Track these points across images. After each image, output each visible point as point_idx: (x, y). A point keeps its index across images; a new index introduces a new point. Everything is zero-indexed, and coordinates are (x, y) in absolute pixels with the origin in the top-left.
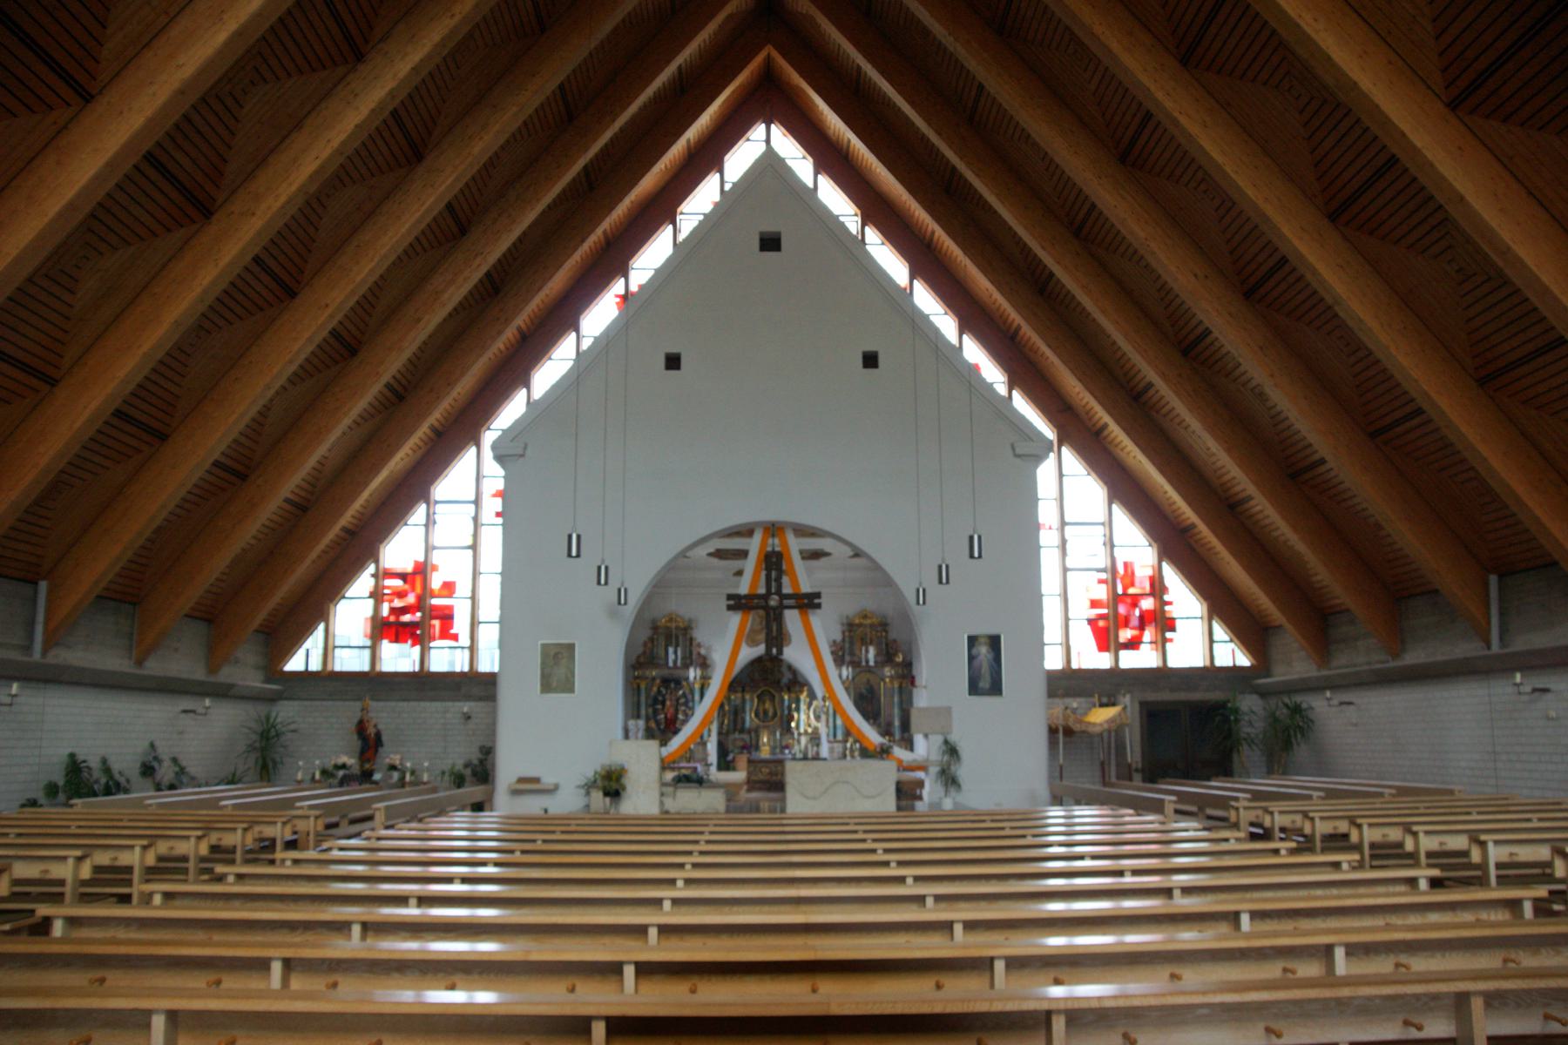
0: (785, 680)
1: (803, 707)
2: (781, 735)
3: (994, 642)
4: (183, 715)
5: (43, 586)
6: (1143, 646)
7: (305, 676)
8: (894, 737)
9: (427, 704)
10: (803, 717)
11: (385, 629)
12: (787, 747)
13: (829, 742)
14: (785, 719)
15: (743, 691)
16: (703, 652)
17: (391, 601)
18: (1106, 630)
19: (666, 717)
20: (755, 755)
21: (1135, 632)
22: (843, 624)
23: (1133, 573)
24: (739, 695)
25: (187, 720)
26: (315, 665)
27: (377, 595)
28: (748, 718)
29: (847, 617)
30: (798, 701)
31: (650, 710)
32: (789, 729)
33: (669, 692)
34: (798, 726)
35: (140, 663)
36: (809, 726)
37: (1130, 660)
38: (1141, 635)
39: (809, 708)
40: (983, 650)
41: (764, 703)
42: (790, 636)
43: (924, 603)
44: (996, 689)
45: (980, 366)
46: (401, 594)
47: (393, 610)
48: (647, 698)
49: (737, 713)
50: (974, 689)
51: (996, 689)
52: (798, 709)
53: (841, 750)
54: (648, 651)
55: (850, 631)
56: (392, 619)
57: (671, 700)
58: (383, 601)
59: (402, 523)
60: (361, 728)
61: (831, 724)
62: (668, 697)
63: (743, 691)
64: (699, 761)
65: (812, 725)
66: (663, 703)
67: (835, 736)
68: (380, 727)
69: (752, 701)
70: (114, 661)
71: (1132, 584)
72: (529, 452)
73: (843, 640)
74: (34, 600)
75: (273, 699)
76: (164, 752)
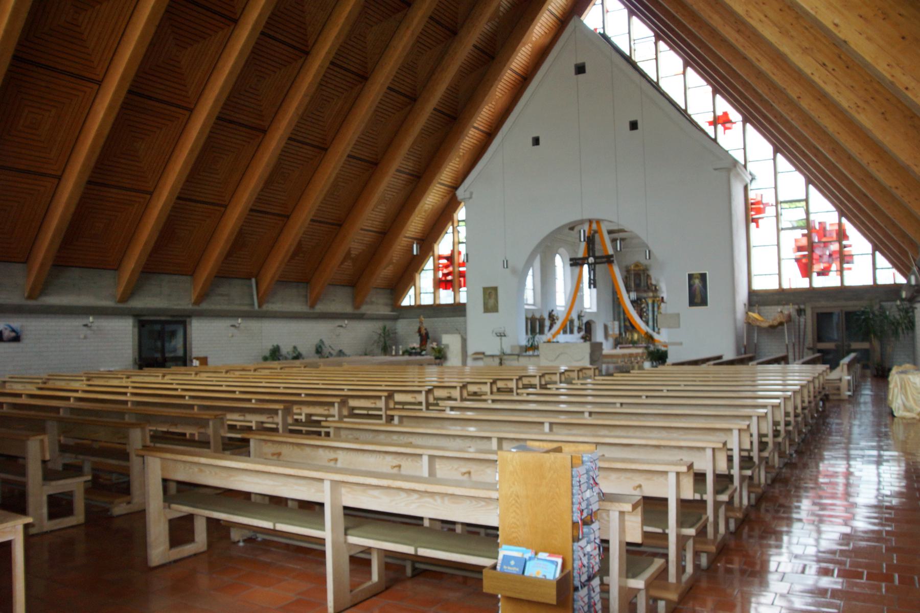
3: (703, 277)
4: (339, 328)
5: (253, 280)
6: (831, 273)
7: (410, 307)
9: (458, 318)
11: (441, 284)
16: (654, 282)
17: (442, 270)
18: (806, 265)
21: (826, 265)
23: (825, 228)
25: (341, 330)
26: (413, 303)
27: (436, 269)
35: (312, 306)
37: (819, 282)
38: (830, 266)
40: (697, 282)
43: (650, 258)
44: (704, 302)
45: (728, 113)
46: (446, 267)
47: (444, 275)
50: (692, 303)
51: (704, 302)
56: (443, 279)
58: (439, 270)
59: (444, 232)
60: (419, 331)
68: (429, 330)
70: (298, 307)
71: (825, 236)
72: (474, 196)
74: (251, 286)
75: (395, 319)
76: (327, 342)
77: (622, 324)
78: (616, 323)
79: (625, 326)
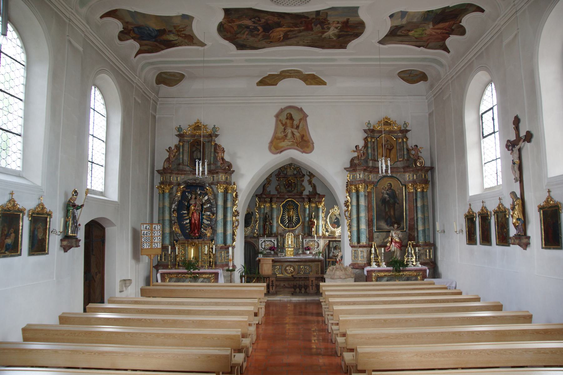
0: (306, 193)
1: (321, 215)
2: (303, 239)
8: (418, 242)
10: (321, 222)
12: (308, 249)
13: (352, 247)
14: (306, 225)
15: (271, 202)
16: (227, 158)
19: (190, 221)
20: (281, 257)
22: (365, 131)
24: (268, 205)
28: (275, 224)
29: (369, 123)
30: (317, 209)
31: (175, 215)
32: (310, 235)
33: (194, 196)
34: (317, 232)
36: (327, 231)
39: (326, 217)
41: (289, 211)
42: (313, 143)
48: (171, 204)
49: (267, 219)
52: (317, 217)
53: (365, 255)
54: (173, 158)
55: (372, 138)
57: (195, 206)
61: (355, 229)
62: (192, 202)
63: (271, 202)
64: (222, 266)
65: (329, 230)
66: (188, 208)
67: (359, 241)
69: (279, 210)
73: (366, 146)
77: (167, 230)
78: (158, 227)
79: (172, 233)
